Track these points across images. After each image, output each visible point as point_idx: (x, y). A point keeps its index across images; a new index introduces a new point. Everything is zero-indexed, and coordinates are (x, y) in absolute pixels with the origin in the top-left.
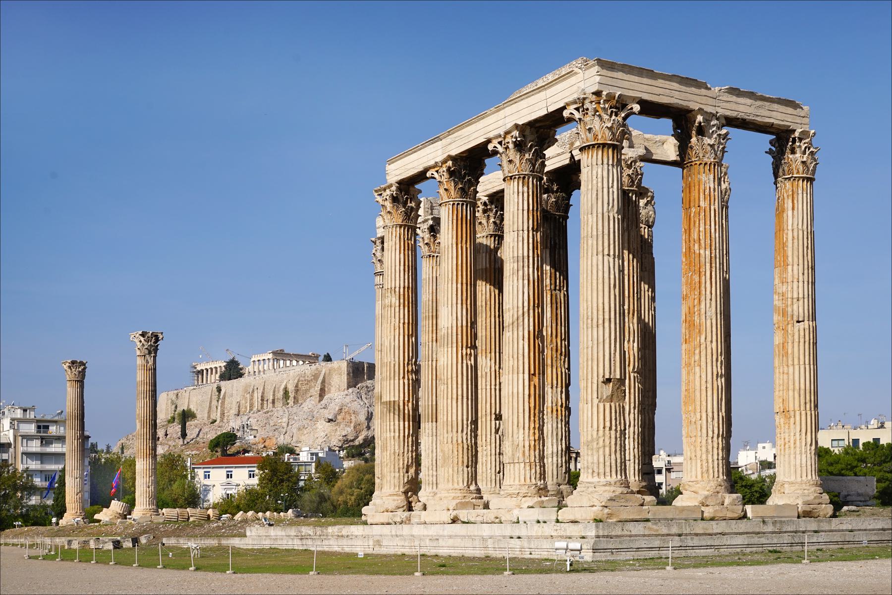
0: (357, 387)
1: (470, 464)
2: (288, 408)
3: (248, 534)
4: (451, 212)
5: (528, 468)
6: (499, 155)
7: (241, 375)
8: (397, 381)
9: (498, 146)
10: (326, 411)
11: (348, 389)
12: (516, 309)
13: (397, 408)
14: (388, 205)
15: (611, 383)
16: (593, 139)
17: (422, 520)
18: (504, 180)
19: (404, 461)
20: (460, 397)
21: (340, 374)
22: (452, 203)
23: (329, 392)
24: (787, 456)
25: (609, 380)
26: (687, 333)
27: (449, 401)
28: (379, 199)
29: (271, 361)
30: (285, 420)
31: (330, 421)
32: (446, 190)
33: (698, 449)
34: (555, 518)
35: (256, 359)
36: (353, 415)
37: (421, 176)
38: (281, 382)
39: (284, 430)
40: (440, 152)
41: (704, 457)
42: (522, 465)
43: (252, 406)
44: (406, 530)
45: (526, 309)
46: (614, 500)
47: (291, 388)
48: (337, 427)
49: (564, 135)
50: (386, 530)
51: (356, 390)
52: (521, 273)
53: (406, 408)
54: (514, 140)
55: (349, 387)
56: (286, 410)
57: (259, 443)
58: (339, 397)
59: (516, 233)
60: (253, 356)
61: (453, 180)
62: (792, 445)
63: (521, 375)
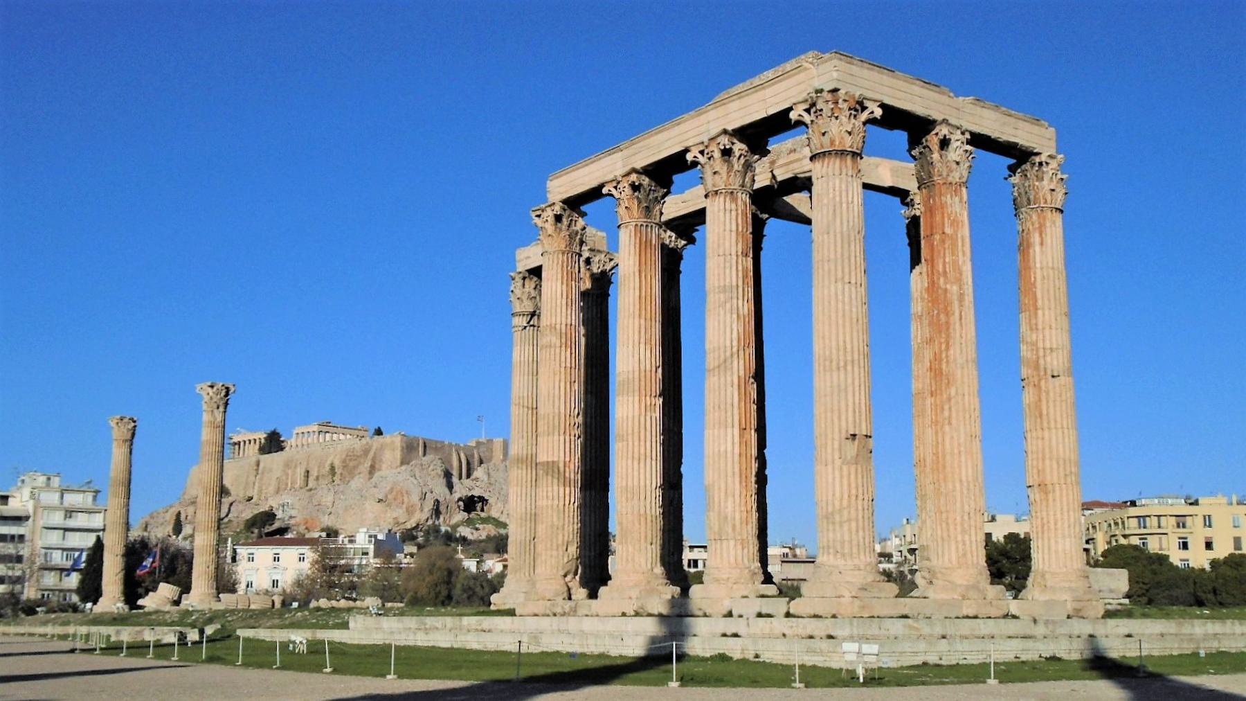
1: (654, 541)
4: (633, 234)
5: (739, 547)
6: (699, 167)
7: (282, 449)
8: (556, 437)
9: (699, 156)
12: (722, 350)
13: (556, 470)
14: (549, 227)
15: (857, 441)
16: (829, 145)
17: (594, 611)
18: (706, 196)
19: (564, 536)
20: (642, 458)
22: (634, 224)
23: (379, 470)
24: (1046, 541)
25: (854, 435)
26: (933, 384)
27: (630, 462)
28: (537, 220)
29: (317, 434)
30: (330, 498)
32: (626, 207)
33: (952, 527)
34: (785, 610)
35: (300, 431)
37: (595, 194)
40: (620, 164)
41: (959, 538)
42: (732, 543)
44: (572, 623)
45: (735, 349)
46: (866, 590)
47: (337, 463)
48: (388, 508)
49: (779, 146)
50: (545, 623)
52: (728, 305)
53: (567, 469)
54: (722, 148)
55: (402, 463)
56: (332, 489)
59: (722, 258)
61: (638, 198)
62: (1052, 526)
63: (729, 430)
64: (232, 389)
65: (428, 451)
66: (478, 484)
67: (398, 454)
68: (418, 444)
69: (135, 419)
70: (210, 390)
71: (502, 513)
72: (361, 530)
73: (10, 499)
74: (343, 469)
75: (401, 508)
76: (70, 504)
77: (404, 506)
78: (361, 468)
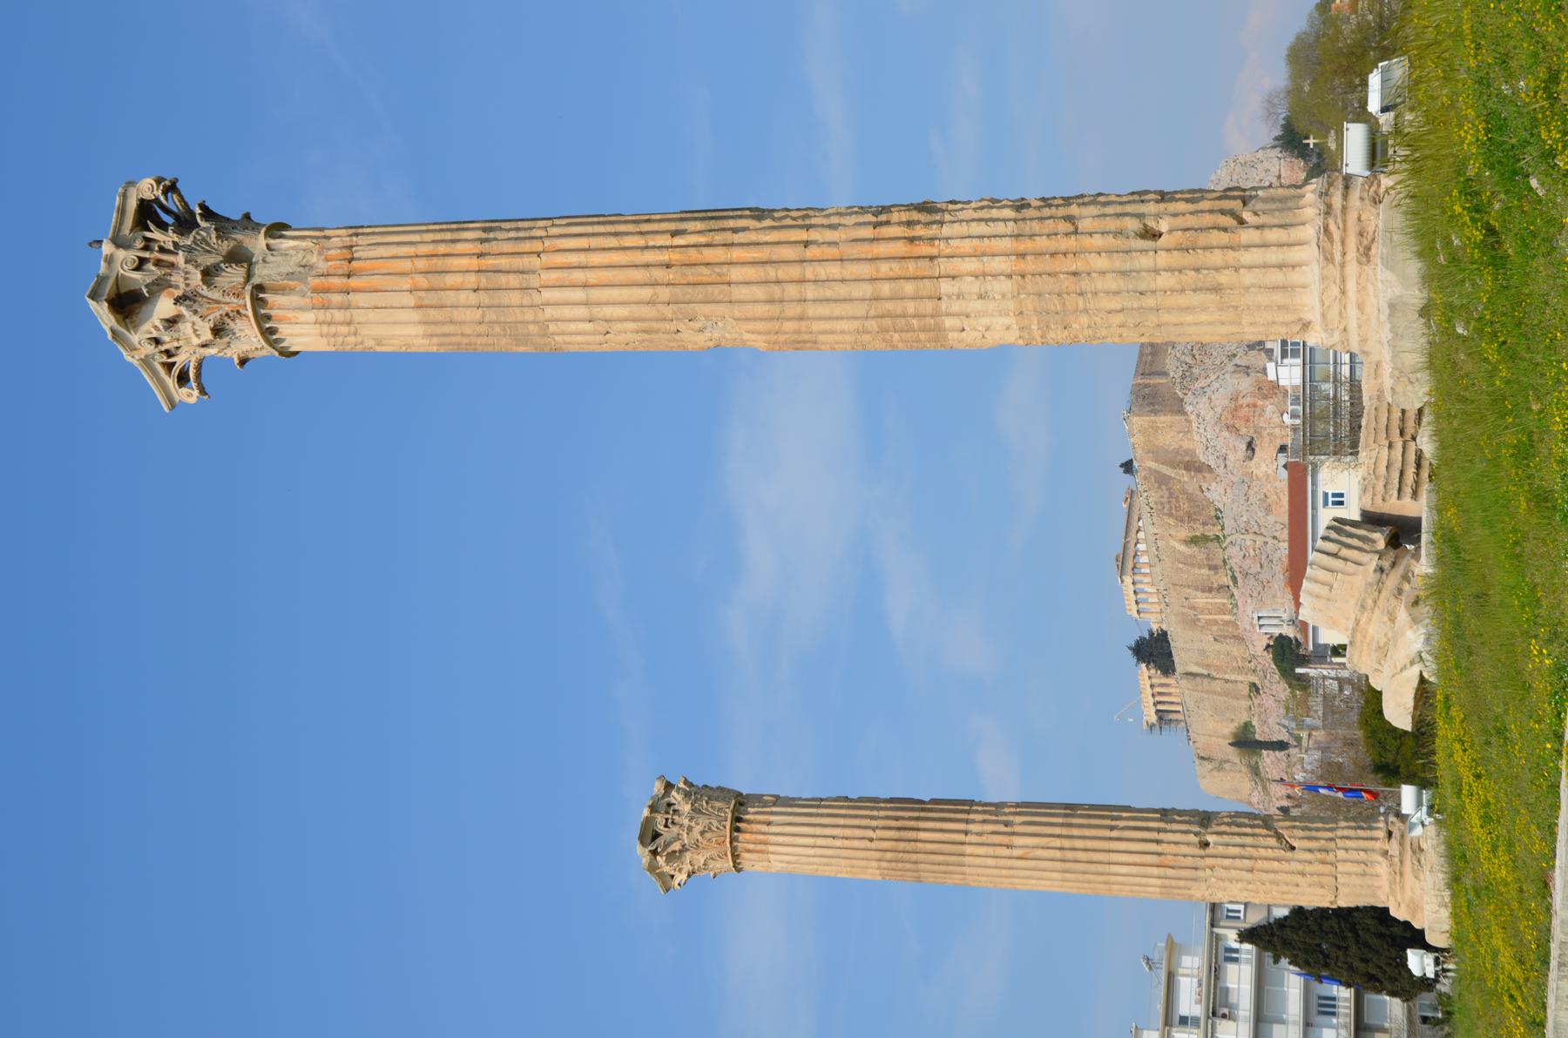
0: (1181, 396)
2: (1224, 536)
10: (1231, 457)
11: (1185, 414)
21: (1156, 429)
23: (1192, 453)
29: (1137, 578)
31: (1250, 446)
35: (1135, 608)
36: (1240, 403)
39: (1270, 541)
43: (1221, 610)
47: (1184, 533)
48: (1265, 433)
51: (1187, 399)
55: (1182, 412)
58: (1202, 431)
60: (1129, 613)
64: (147, 188)
65: (1159, 369)
67: (1163, 419)
68: (1146, 386)
69: (658, 788)
72: (1271, 376)
74: (1195, 521)
76: (1200, 1002)
77: (1260, 403)
78: (1192, 488)
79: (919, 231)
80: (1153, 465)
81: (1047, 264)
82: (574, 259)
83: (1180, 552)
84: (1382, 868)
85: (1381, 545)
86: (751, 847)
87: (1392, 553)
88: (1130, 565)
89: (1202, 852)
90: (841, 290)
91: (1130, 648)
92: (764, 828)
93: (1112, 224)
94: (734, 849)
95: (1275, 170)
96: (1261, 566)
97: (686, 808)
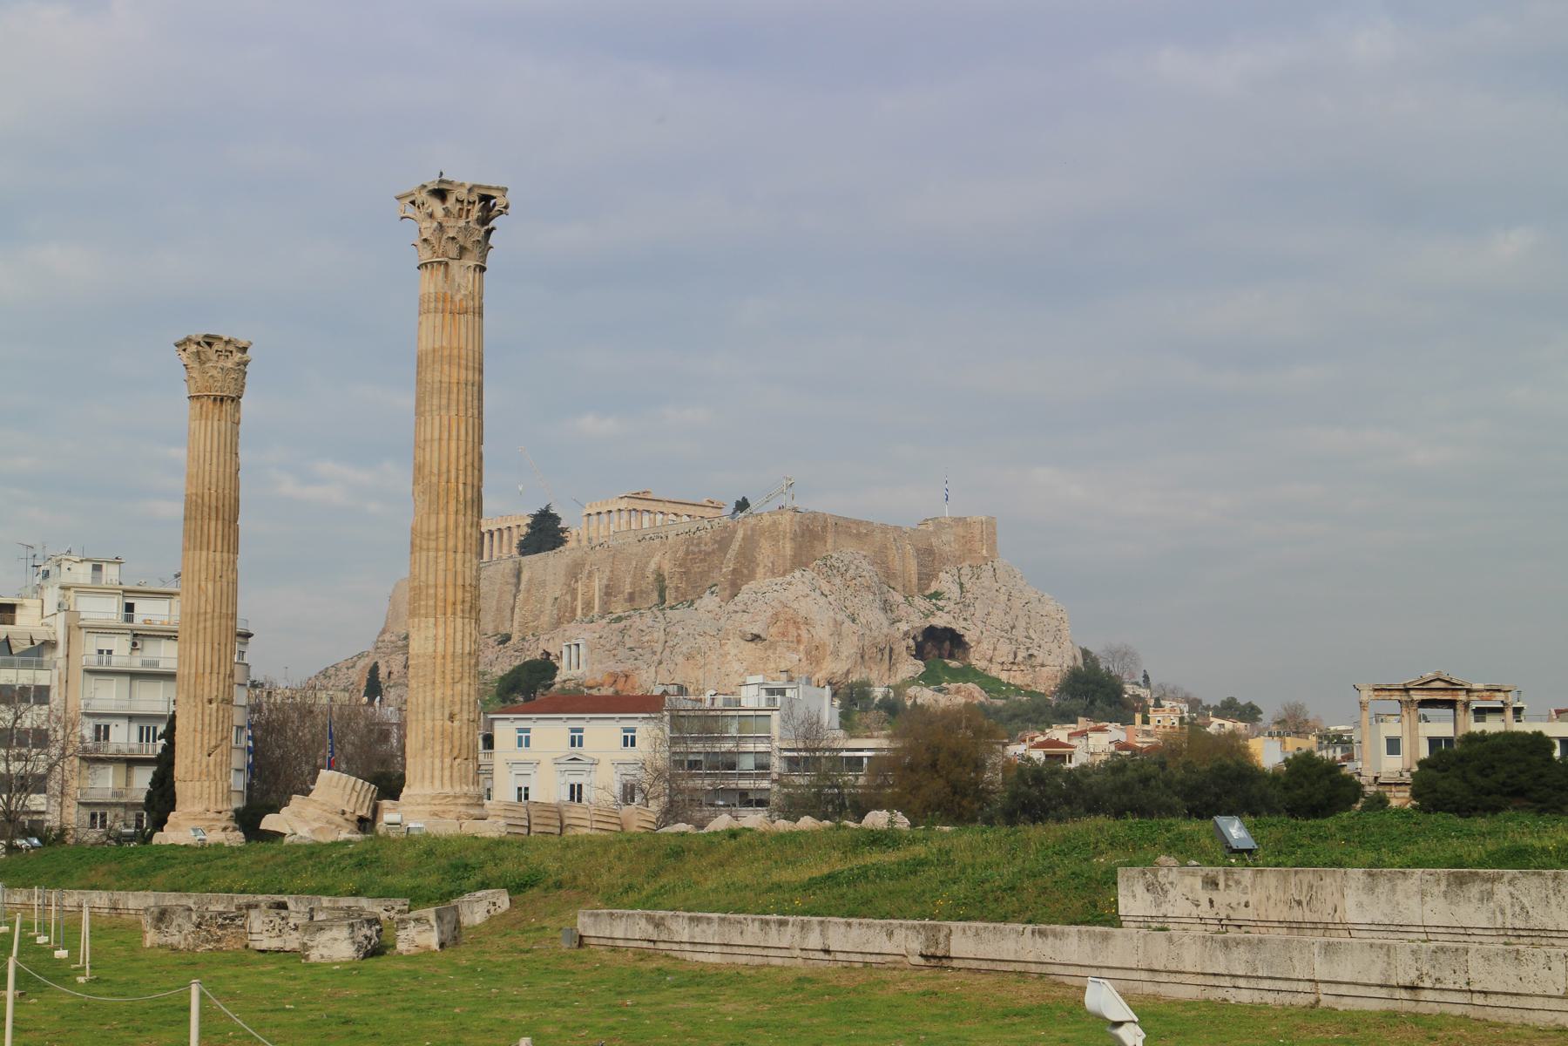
2: (663, 609)
3: (1132, 899)
7: (562, 542)
11: (792, 570)
23: (751, 576)
29: (625, 515)
31: (756, 638)
38: (651, 556)
43: (588, 606)
47: (667, 568)
48: (770, 652)
57: (602, 685)
58: (775, 587)
64: (500, 202)
66: (940, 603)
67: (788, 548)
69: (243, 342)
70: (436, 206)
71: (991, 661)
72: (750, 680)
73: (18, 611)
74: (681, 579)
75: (796, 651)
77: (802, 648)
78: (716, 576)
79: (459, 607)
80: (740, 534)
81: (439, 670)
82: (454, 433)
83: (647, 563)
84: (199, 808)
85: (359, 813)
86: (204, 409)
87: (355, 818)
88: (640, 505)
89: (205, 700)
90: (432, 570)
91: (548, 507)
92: (216, 417)
93: (457, 699)
94: (203, 397)
95: (1049, 660)
96: (631, 649)
97: (229, 365)
